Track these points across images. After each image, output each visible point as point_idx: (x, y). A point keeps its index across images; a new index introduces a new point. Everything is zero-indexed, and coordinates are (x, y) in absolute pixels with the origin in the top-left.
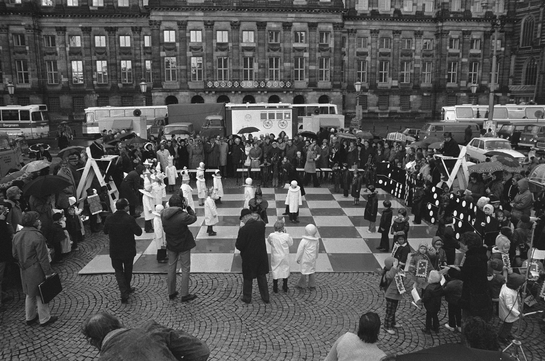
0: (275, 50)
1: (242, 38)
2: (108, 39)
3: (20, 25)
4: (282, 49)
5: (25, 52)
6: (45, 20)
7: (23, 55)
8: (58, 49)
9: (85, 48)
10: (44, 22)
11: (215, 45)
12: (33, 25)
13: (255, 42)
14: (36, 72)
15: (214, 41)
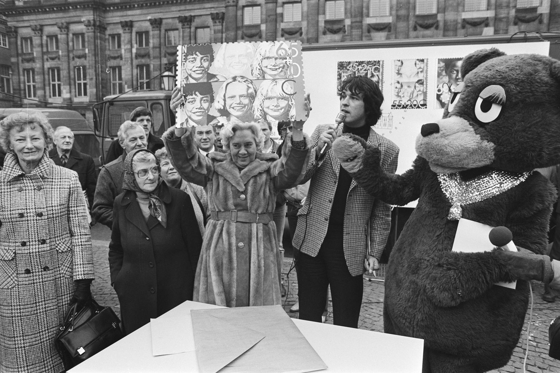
0: (427, 27)
1: (368, 8)
2: (181, 34)
3: (80, 22)
4: (441, 24)
5: (84, 56)
6: (110, 14)
7: (83, 59)
8: (123, 51)
9: (154, 47)
10: (108, 17)
11: (322, 24)
12: (94, 20)
13: (391, 14)
14: (94, 81)
15: (321, 19)
